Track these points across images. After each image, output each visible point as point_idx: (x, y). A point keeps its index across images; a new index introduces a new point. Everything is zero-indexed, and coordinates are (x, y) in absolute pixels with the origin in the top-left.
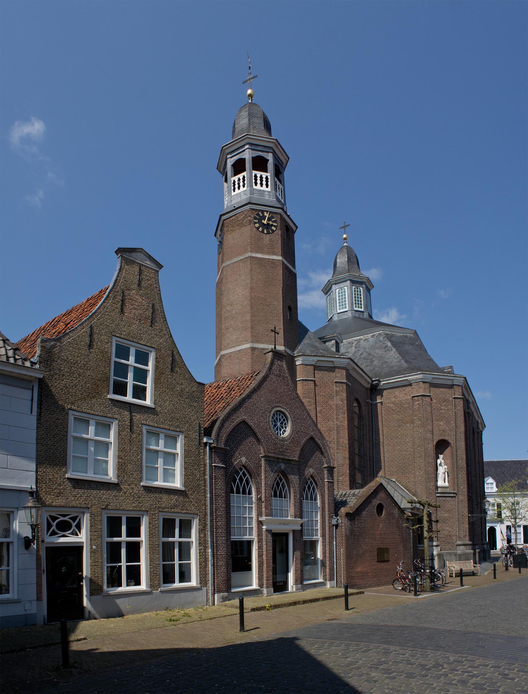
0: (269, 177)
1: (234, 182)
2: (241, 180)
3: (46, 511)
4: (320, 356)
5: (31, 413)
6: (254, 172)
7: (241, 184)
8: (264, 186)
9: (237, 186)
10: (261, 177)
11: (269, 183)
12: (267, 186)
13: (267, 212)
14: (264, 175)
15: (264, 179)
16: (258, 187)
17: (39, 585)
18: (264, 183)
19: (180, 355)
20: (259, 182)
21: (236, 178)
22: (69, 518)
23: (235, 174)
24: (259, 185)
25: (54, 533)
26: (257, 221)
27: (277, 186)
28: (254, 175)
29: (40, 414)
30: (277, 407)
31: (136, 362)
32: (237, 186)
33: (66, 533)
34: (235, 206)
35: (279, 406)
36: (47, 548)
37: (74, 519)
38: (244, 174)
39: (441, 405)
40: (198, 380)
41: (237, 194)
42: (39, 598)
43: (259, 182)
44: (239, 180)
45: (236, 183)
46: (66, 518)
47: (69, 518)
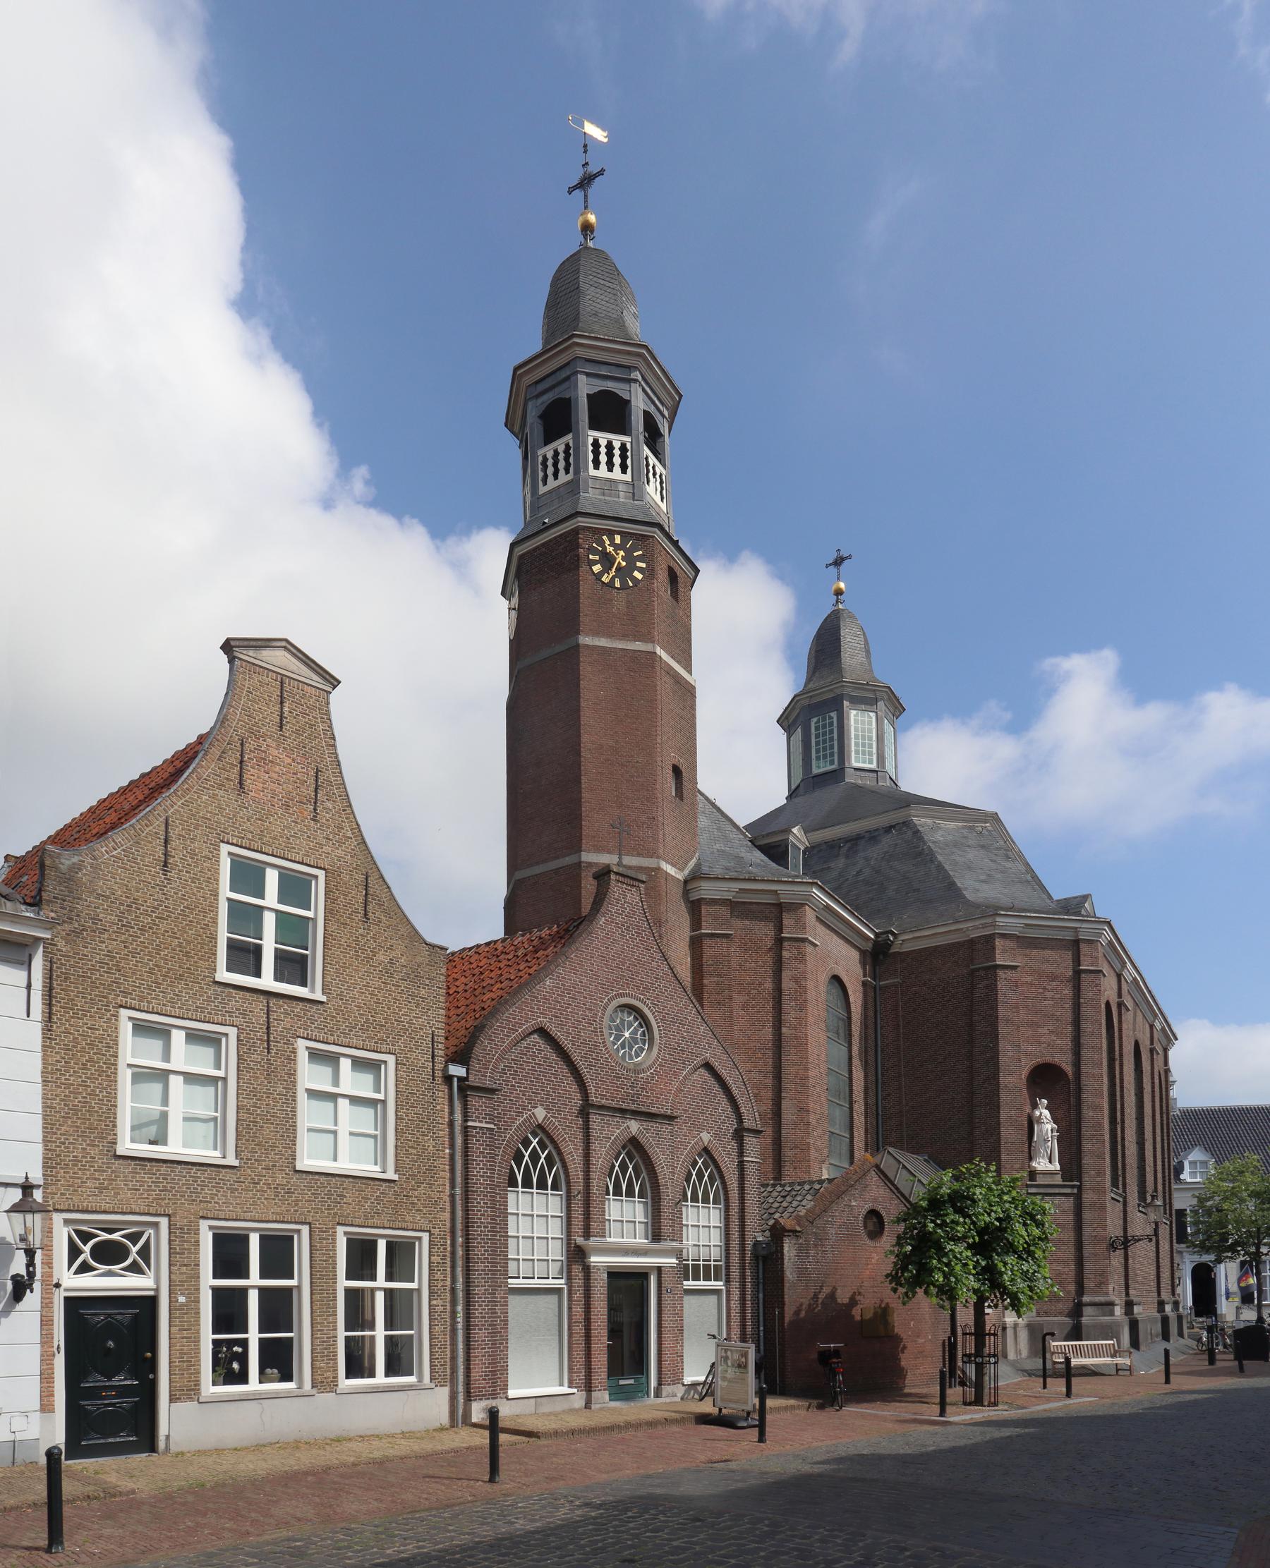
0: (628, 446)
1: (545, 459)
2: (561, 456)
3: (67, 1222)
4: (731, 879)
5: (28, 1016)
7: (562, 465)
8: (617, 468)
9: (550, 470)
10: (610, 446)
11: (629, 462)
13: (619, 533)
14: (617, 439)
15: (617, 452)
16: (603, 472)
17: (46, 1378)
18: (617, 460)
19: (386, 884)
20: (603, 458)
21: (548, 451)
22: (123, 1236)
23: (548, 439)
24: (603, 466)
25: (85, 1268)
26: (597, 558)
27: (650, 468)
28: (591, 440)
29: (49, 1017)
30: (622, 995)
31: (280, 902)
32: (550, 470)
33: (115, 1268)
34: (546, 521)
35: (627, 995)
36: (67, 1299)
37: (134, 1238)
38: (569, 438)
39: (1045, 988)
40: (429, 940)
41: (550, 492)
42: (46, 1407)
43: (603, 458)
44: (556, 453)
45: (550, 462)
46: (116, 1236)
47: (123, 1236)
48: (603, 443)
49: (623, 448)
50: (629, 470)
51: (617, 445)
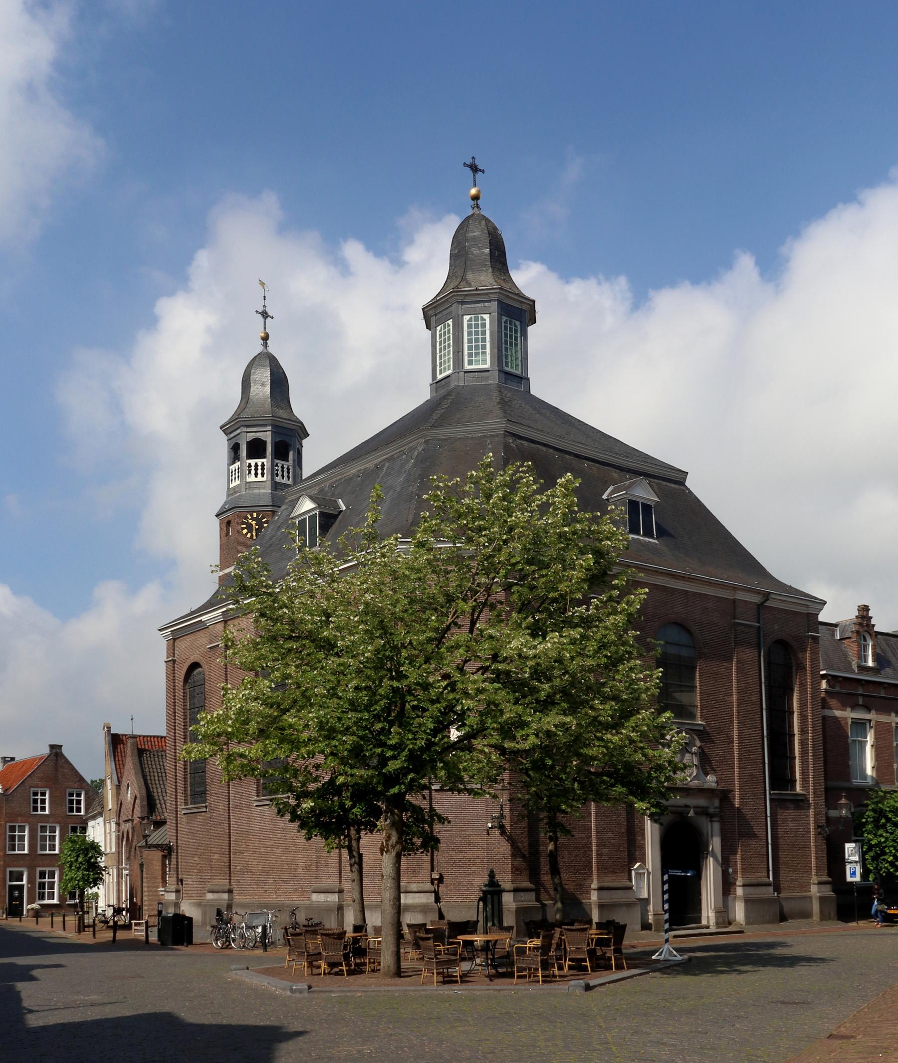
0: (265, 463)
6: (249, 461)
10: (256, 465)
11: (265, 471)
12: (263, 475)
14: (259, 461)
15: (259, 468)
18: (259, 471)
26: (244, 526)
48: (253, 464)
49: (263, 465)
50: (265, 475)
51: (260, 464)
